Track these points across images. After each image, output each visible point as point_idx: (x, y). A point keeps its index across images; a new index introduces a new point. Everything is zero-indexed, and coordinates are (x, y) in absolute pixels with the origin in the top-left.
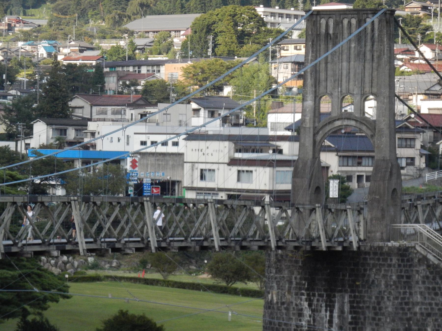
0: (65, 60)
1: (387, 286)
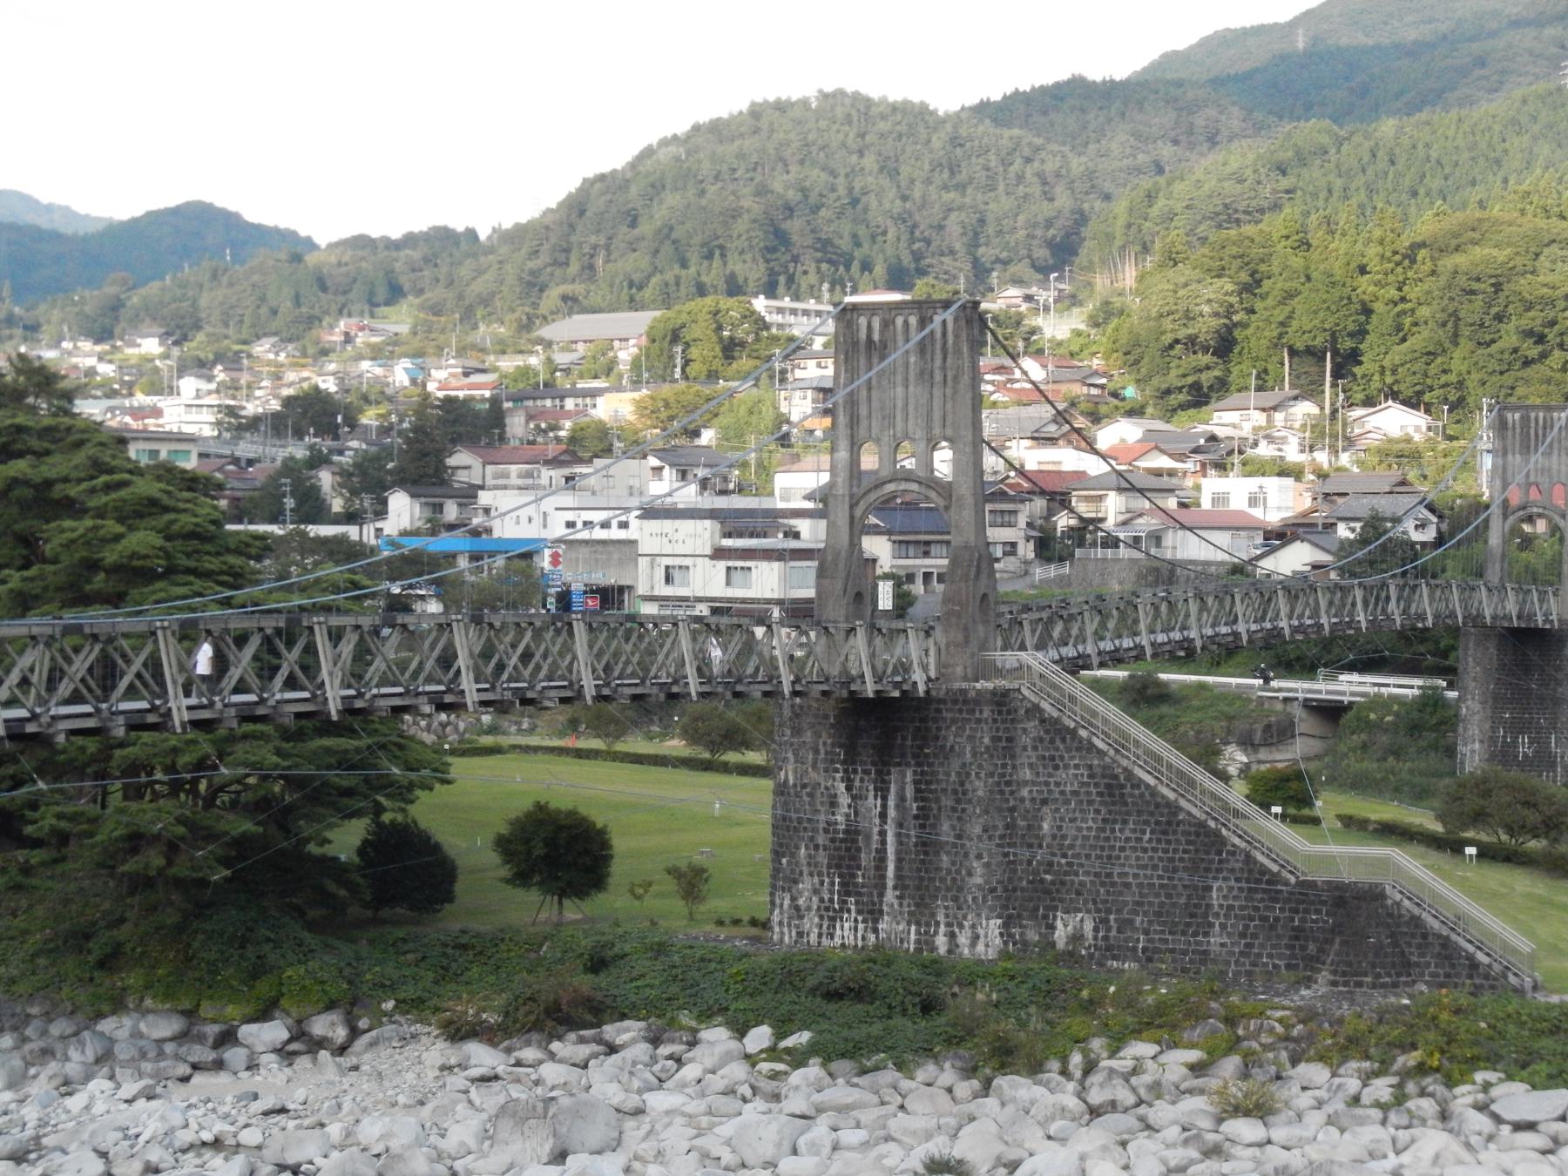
0: (439, 389)
1: (974, 755)
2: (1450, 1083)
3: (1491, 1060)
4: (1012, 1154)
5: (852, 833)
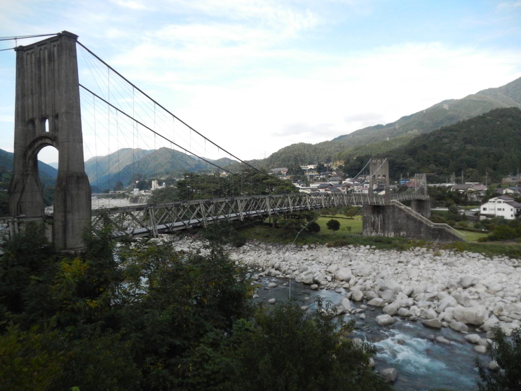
2: (462, 252)
3: (466, 249)
4: (409, 261)
5: (374, 222)
